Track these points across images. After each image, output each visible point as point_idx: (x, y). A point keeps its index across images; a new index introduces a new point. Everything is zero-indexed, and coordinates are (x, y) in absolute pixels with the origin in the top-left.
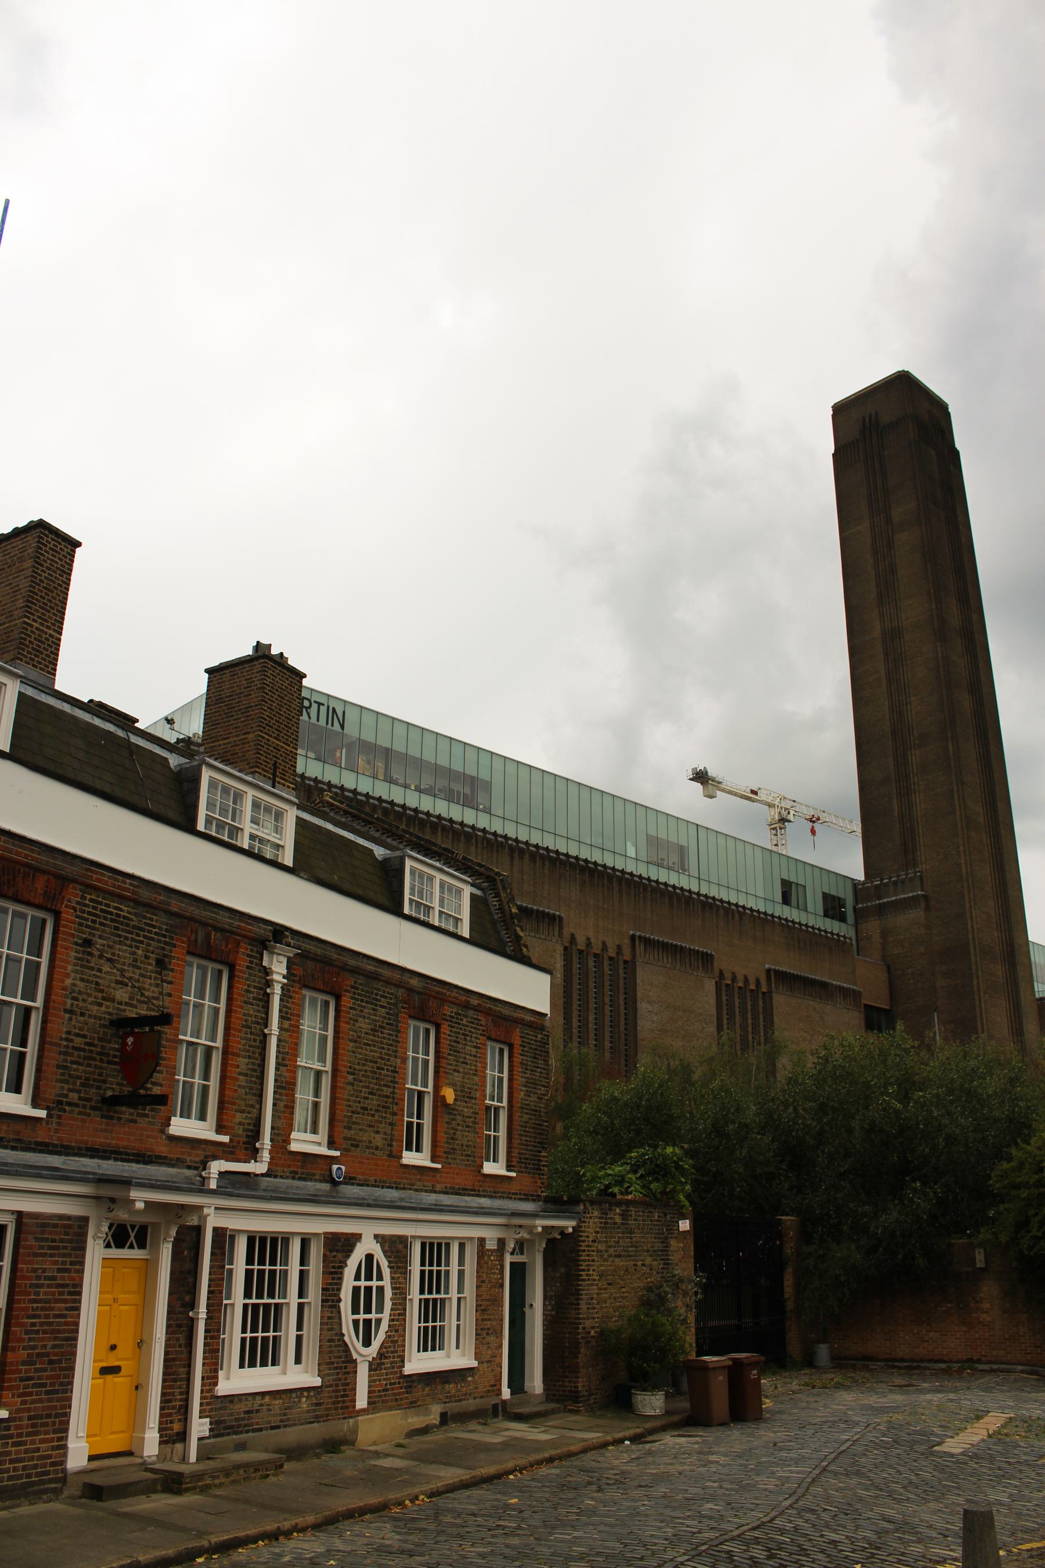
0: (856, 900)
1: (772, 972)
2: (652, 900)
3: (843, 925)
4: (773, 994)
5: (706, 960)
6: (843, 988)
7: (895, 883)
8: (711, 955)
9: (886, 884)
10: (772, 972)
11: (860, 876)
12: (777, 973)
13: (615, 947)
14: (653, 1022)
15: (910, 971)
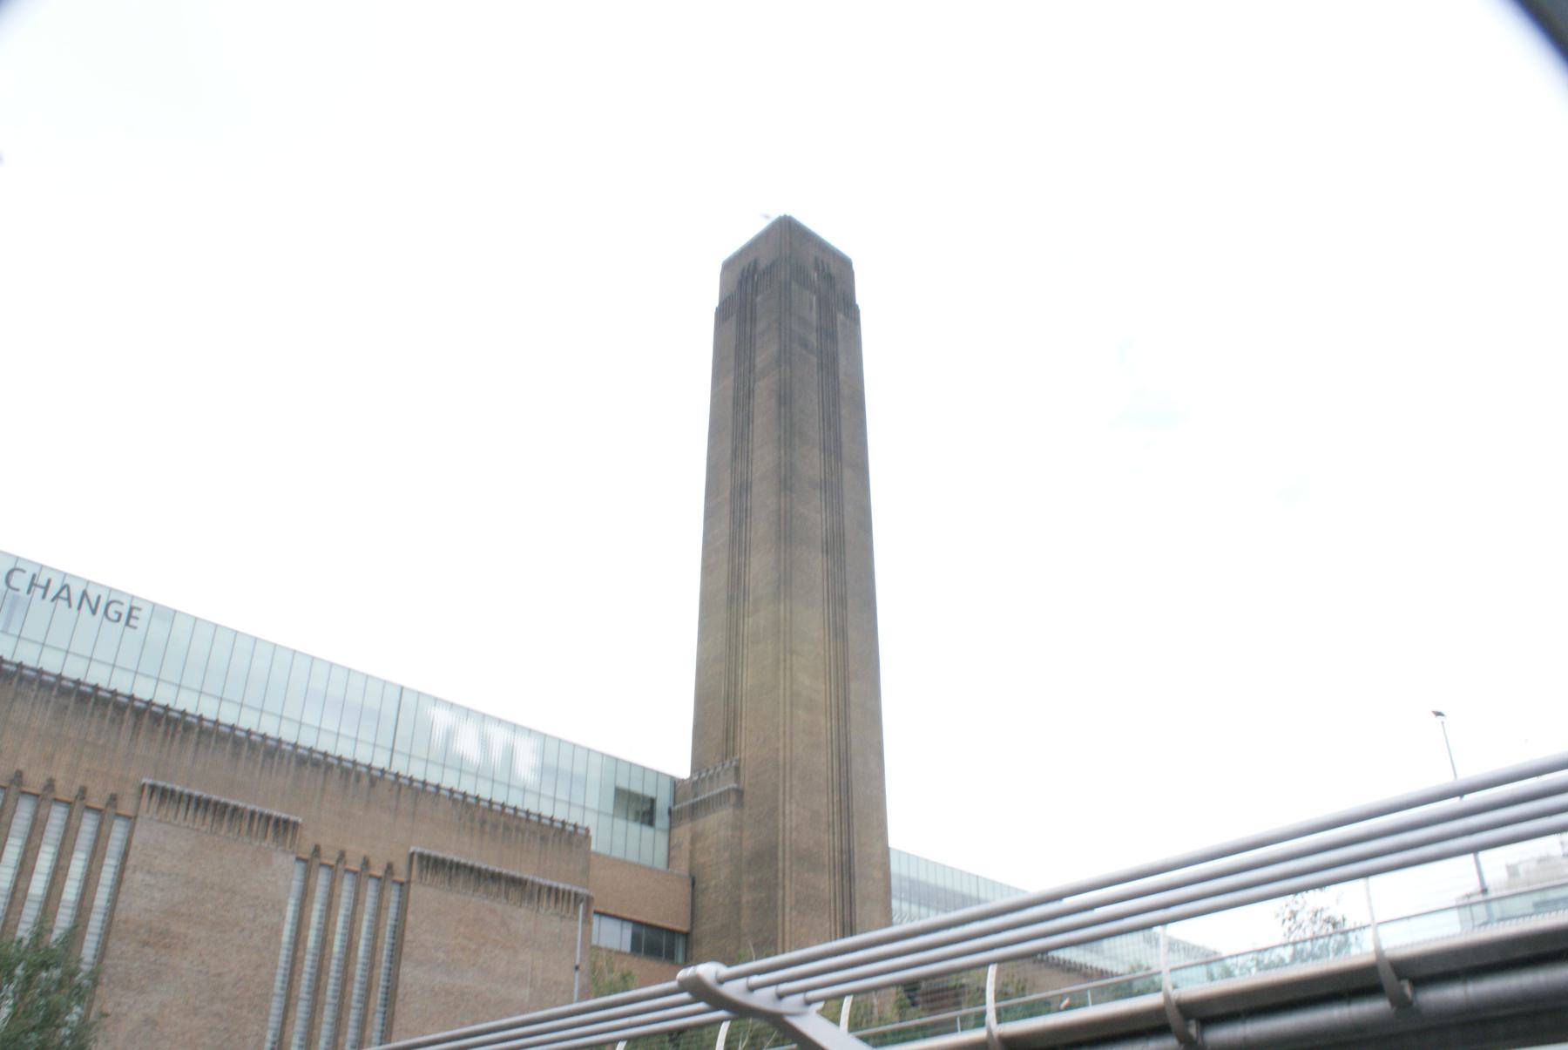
0: (675, 801)
1: (416, 857)
2: (198, 744)
3: (647, 831)
4: (412, 885)
5: (283, 827)
6: (557, 890)
7: (711, 778)
8: (295, 824)
9: (703, 780)
10: (416, 857)
11: (680, 766)
12: (421, 856)
13: (106, 796)
14: (153, 899)
15: (713, 883)
